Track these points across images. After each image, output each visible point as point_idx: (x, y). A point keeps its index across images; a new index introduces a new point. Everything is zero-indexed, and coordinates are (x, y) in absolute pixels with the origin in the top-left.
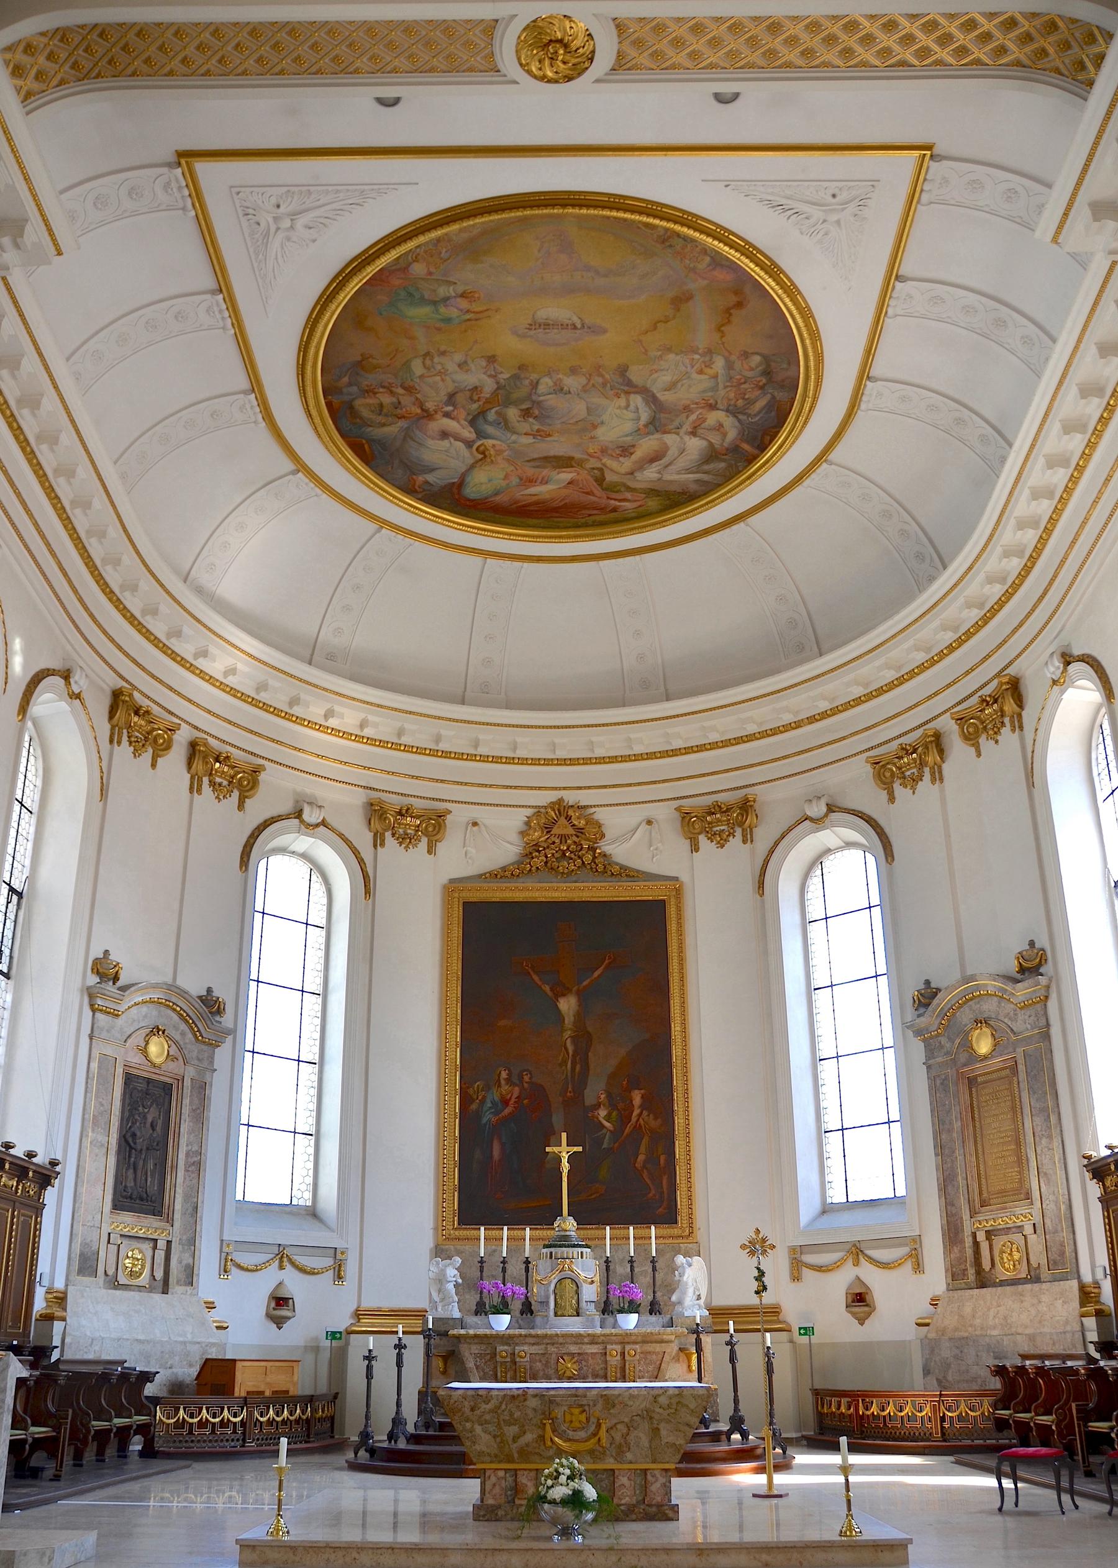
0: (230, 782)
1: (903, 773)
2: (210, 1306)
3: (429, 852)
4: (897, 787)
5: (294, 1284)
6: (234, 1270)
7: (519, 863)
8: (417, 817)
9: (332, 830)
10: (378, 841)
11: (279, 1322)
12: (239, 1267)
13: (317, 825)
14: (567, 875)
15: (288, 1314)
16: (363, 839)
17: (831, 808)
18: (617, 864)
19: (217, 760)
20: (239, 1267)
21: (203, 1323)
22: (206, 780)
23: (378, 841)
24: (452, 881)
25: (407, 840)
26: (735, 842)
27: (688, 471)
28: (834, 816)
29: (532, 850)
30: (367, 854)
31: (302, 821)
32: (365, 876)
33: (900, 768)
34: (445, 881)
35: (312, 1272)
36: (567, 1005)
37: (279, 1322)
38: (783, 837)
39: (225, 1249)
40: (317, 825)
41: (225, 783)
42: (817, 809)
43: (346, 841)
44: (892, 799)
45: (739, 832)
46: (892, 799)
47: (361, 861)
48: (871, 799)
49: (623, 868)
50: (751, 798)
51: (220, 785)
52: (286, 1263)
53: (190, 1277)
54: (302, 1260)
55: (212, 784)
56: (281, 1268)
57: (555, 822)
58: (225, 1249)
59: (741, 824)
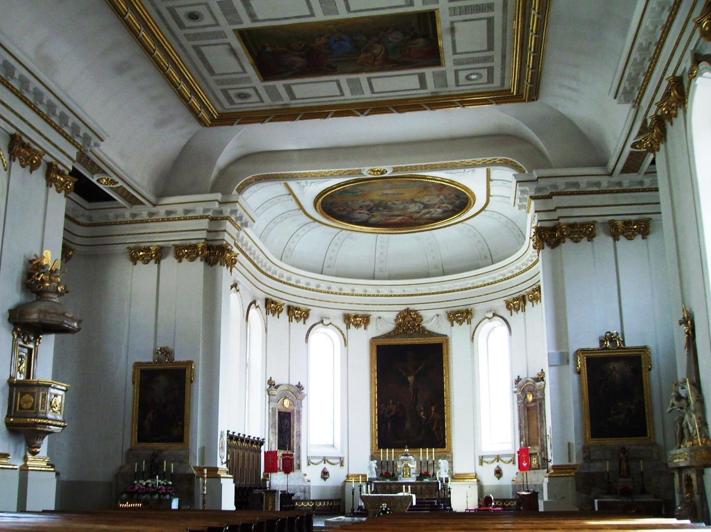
0: (301, 316)
1: (515, 307)
2: (305, 475)
3: (365, 329)
4: (513, 310)
5: (329, 468)
6: (311, 464)
7: (394, 331)
8: (360, 318)
9: (333, 325)
10: (348, 327)
11: (325, 479)
12: (313, 463)
13: (328, 325)
14: (411, 336)
15: (328, 476)
16: (343, 327)
17: (494, 315)
18: (427, 330)
19: (296, 310)
20: (313, 463)
21: (303, 480)
22: (293, 317)
23: (348, 327)
24: (373, 338)
25: (357, 326)
26: (465, 324)
27: (440, 214)
28: (495, 318)
29: (399, 326)
30: (344, 331)
31: (323, 324)
32: (345, 340)
33: (513, 305)
34: (370, 338)
35: (334, 464)
36: (411, 379)
37: (325, 479)
38: (480, 323)
39: (309, 459)
40: (328, 325)
41: (299, 316)
42: (490, 315)
43: (338, 328)
44: (511, 315)
45: (466, 320)
46: (511, 315)
47: (343, 334)
48: (505, 313)
49: (429, 332)
50: (470, 309)
51: (298, 317)
52: (326, 462)
53: (299, 467)
54: (331, 461)
55: (295, 318)
56: (325, 463)
57: (406, 316)
58: (309, 459)
59: (467, 318)
